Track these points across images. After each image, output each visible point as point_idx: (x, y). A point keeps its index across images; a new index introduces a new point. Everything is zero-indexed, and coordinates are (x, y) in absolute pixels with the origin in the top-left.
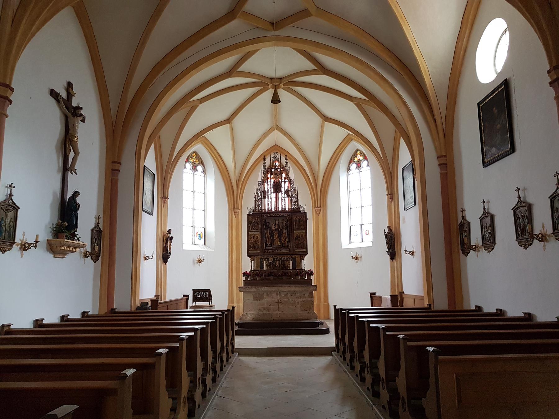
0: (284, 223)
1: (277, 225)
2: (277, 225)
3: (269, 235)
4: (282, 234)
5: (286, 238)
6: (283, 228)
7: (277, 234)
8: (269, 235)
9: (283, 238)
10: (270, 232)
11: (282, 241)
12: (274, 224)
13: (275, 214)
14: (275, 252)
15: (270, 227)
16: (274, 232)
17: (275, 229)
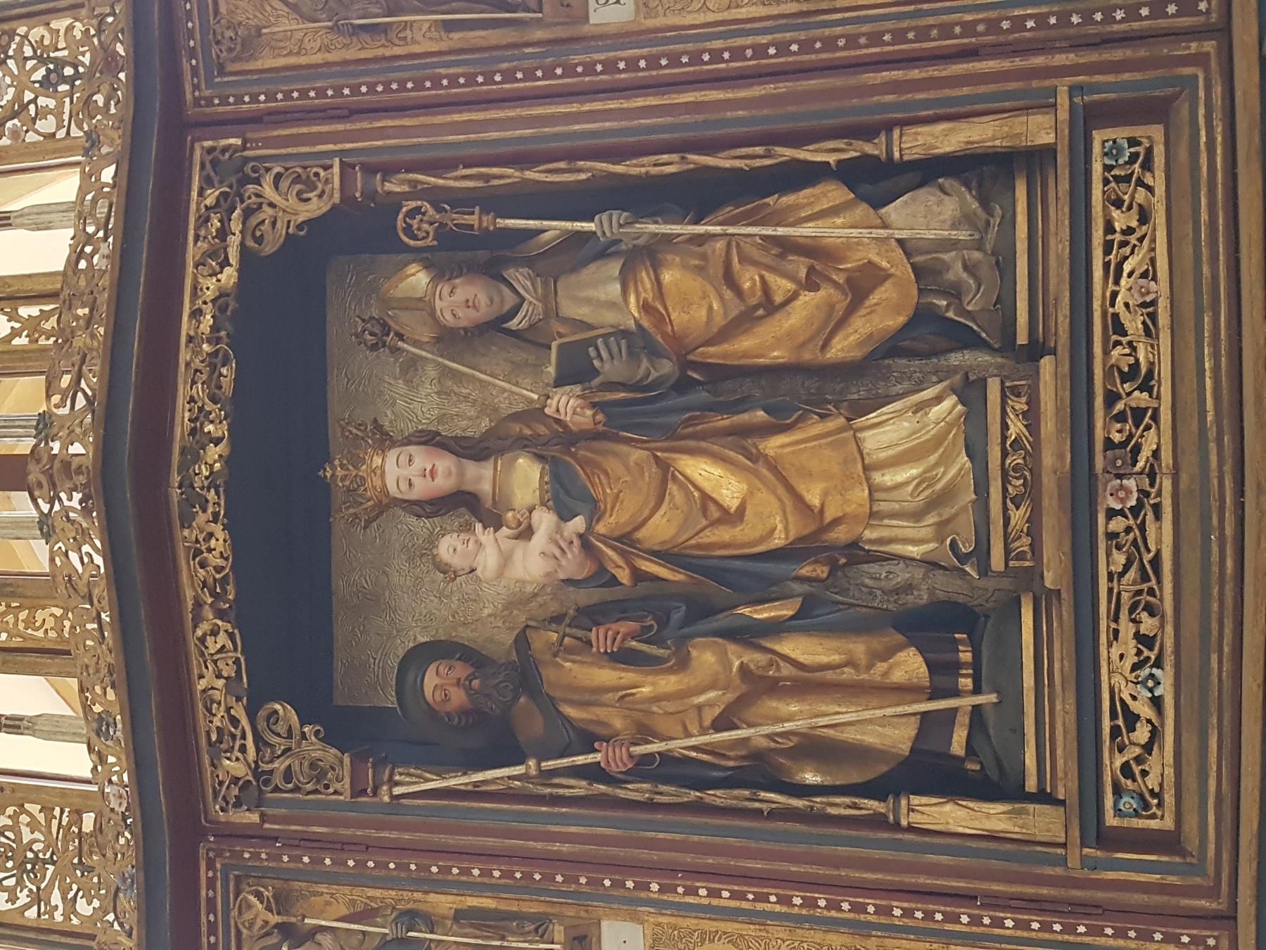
0: (423, 305)
1: (481, 477)
2: (481, 477)
3: (683, 664)
4: (681, 348)
5: (787, 247)
6: (533, 339)
7: (665, 469)
8: (683, 664)
9: (770, 306)
10: (601, 637)
11: (843, 347)
12: (450, 548)
13: (193, 501)
14: (1161, 536)
15: (522, 641)
16: (626, 541)
17: (544, 521)
